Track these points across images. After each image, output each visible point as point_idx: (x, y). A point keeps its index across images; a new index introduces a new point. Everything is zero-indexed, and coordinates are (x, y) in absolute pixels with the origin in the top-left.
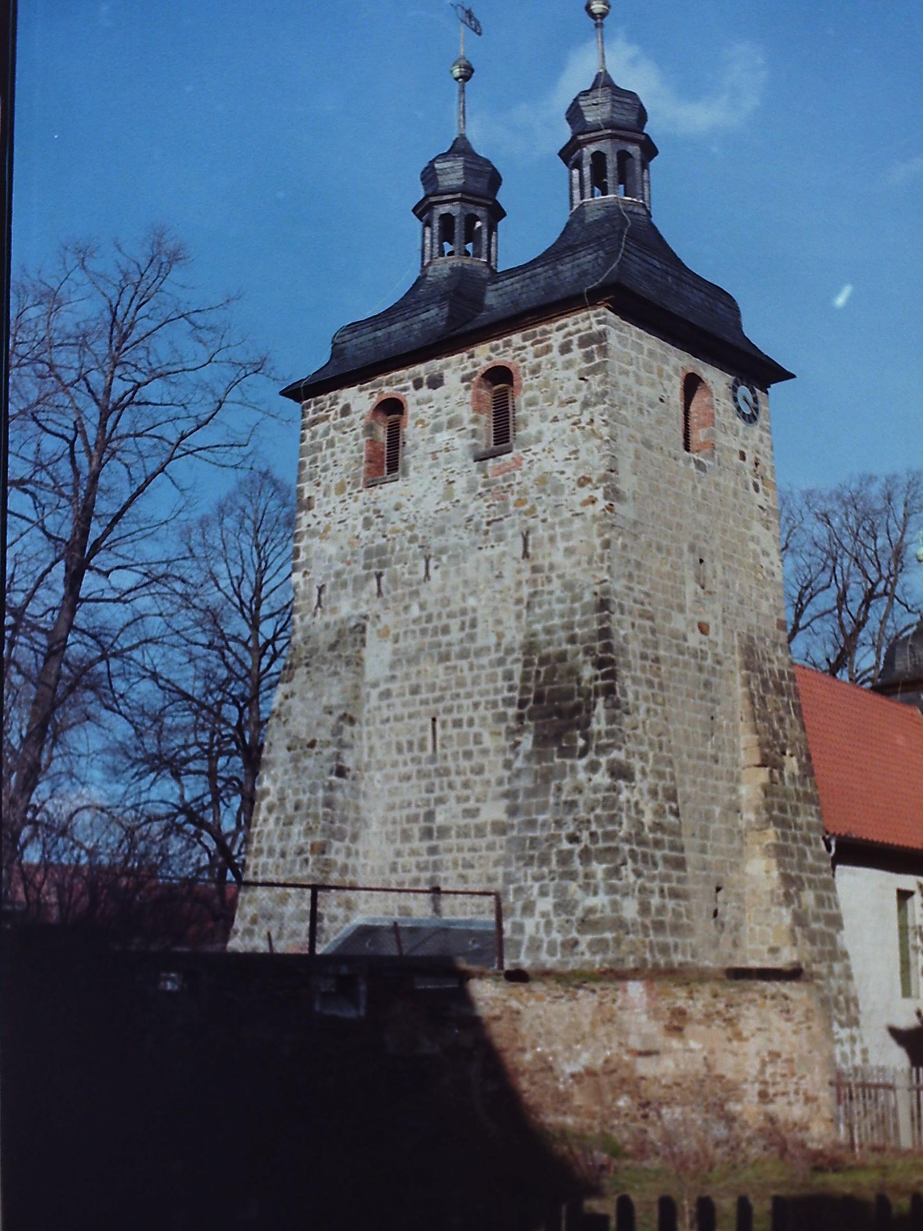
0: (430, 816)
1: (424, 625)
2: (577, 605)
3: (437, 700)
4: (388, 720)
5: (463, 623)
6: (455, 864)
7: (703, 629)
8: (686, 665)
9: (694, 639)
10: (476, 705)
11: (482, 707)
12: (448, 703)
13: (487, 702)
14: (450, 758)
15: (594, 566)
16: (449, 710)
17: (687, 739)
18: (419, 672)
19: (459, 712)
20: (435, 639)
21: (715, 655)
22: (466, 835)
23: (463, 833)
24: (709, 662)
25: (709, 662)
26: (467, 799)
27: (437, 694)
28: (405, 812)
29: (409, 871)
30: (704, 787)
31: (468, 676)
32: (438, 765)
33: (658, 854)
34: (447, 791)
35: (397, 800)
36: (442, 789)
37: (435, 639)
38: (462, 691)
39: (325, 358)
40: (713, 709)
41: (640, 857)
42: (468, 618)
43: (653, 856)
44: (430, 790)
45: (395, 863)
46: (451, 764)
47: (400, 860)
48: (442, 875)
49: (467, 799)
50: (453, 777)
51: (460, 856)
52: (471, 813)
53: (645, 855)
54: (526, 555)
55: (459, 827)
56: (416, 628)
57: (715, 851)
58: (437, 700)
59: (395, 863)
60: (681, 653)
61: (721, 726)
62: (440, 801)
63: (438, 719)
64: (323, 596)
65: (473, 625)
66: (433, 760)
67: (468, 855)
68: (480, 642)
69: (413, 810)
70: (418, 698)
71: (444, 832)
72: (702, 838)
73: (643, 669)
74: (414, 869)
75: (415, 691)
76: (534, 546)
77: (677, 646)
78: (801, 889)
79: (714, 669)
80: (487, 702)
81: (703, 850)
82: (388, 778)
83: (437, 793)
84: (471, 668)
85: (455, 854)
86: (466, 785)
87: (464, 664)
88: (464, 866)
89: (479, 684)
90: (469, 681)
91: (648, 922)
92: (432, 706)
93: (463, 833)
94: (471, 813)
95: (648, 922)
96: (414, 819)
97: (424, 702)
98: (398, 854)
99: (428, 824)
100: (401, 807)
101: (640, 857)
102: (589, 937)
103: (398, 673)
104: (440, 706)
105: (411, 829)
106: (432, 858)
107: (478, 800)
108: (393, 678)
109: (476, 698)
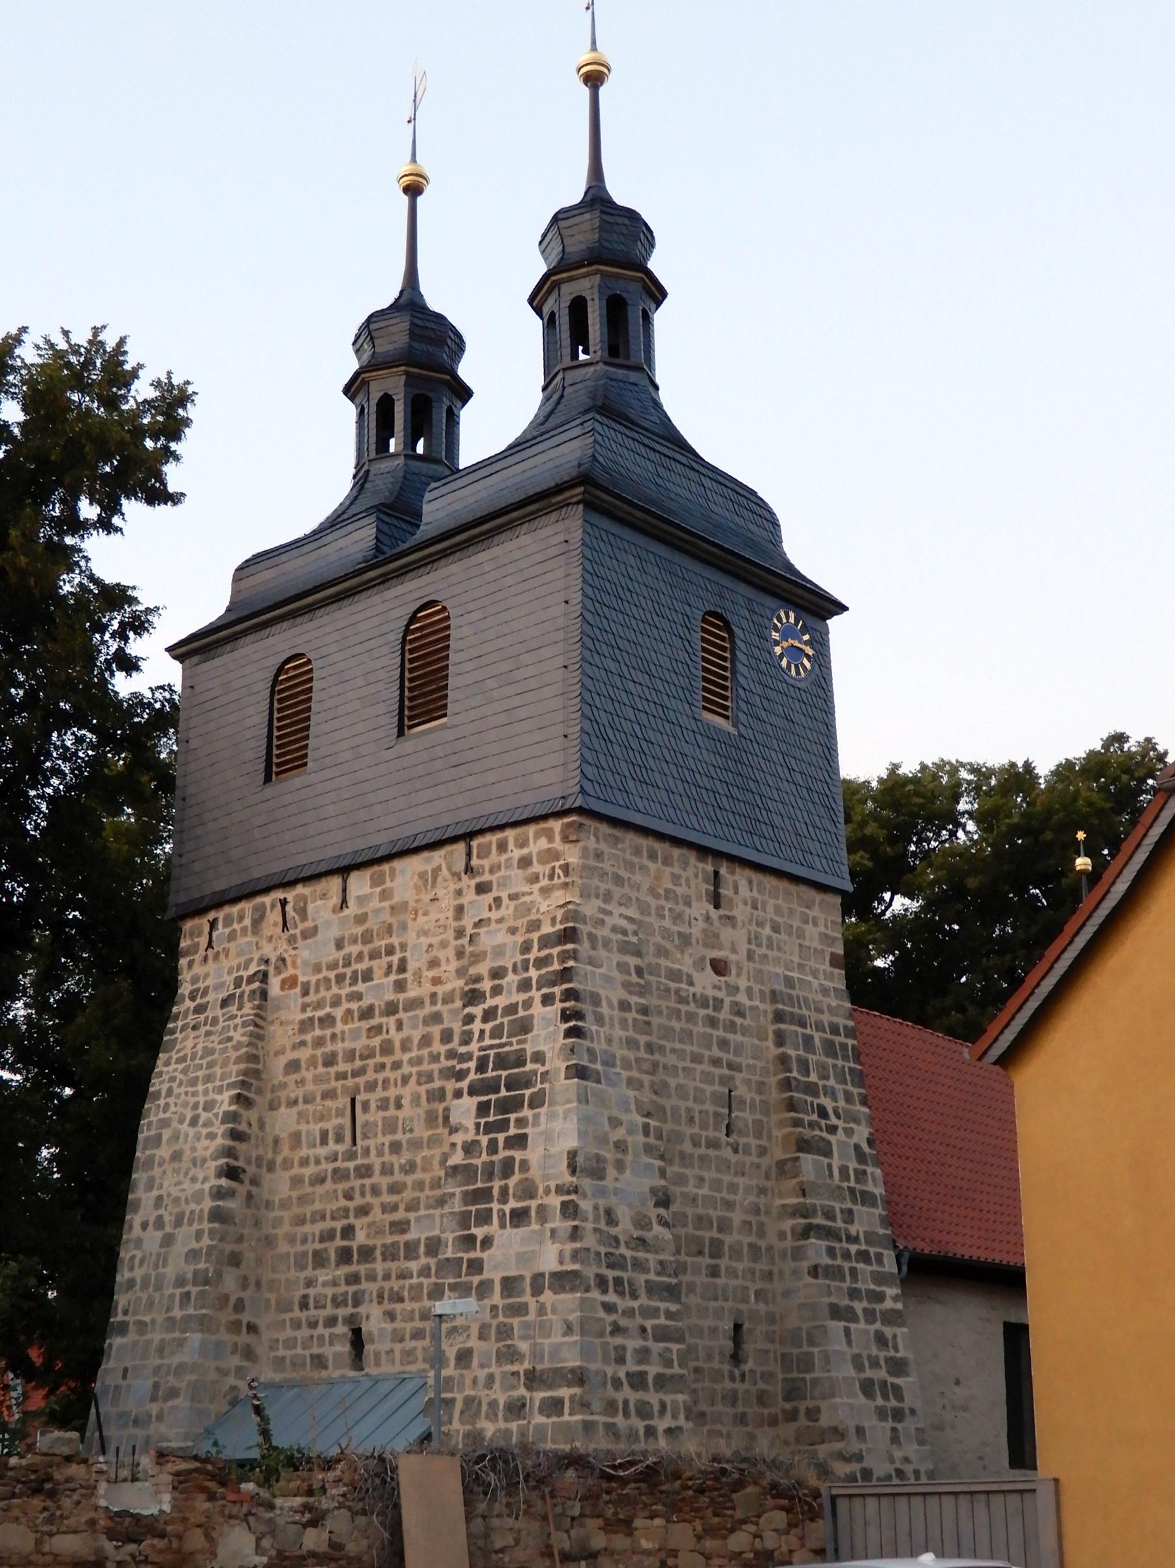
0: (348, 1232)
1: (341, 970)
2: (535, 936)
3: (356, 1074)
4: (295, 1102)
5: (390, 966)
6: (380, 1297)
7: (719, 968)
8: (691, 1017)
9: (706, 981)
10: (405, 1080)
11: (413, 1080)
12: (370, 1075)
13: (419, 1074)
14: (373, 1152)
15: (556, 881)
16: (371, 1087)
17: (691, 1120)
18: (334, 1036)
19: (384, 1089)
20: (354, 988)
21: (736, 1004)
22: (394, 1257)
23: (390, 1254)
24: (724, 1015)
25: (724, 1015)
26: (395, 1208)
27: (358, 1063)
28: (319, 1227)
29: (324, 1307)
30: (716, 1185)
31: (396, 1037)
32: (359, 1162)
33: (641, 1278)
34: (369, 1198)
35: (308, 1210)
36: (363, 1194)
37: (354, 988)
38: (388, 1060)
39: (222, 611)
40: (732, 1078)
41: (611, 1284)
42: (395, 959)
43: (630, 1284)
44: (348, 1196)
45: (305, 1297)
46: (375, 1160)
47: (311, 1292)
48: (362, 1310)
49: (395, 1208)
50: (376, 1179)
51: (387, 1285)
52: (401, 1227)
53: (618, 1282)
54: (469, 870)
55: (384, 1245)
56: (332, 975)
57: (732, 1273)
58: (356, 1074)
59: (305, 1297)
60: (682, 1000)
61: (744, 1102)
62: (363, 1211)
63: (358, 1098)
64: (214, 934)
65: (402, 968)
66: (351, 1156)
67: (395, 1284)
68: (412, 993)
69: (328, 1224)
70: (333, 1070)
71: (366, 1253)
72: (712, 1256)
73: (624, 1023)
74: (329, 1305)
75: (330, 1061)
76: (478, 857)
77: (677, 992)
78: (49, 1479)
79: (733, 1023)
80: (419, 1074)
81: (714, 1272)
82: (297, 1181)
83: (358, 1201)
84: (400, 1026)
85: (380, 1283)
86: (394, 1189)
87: (391, 1021)
88: (391, 1300)
89: (410, 1050)
90: (397, 1045)
91: (622, 1375)
92: (350, 1082)
93: (390, 1254)
94: (401, 1227)
95: (622, 1375)
96: (328, 1236)
97: (342, 1076)
98: (310, 1283)
99: (345, 1243)
100: (313, 1221)
101: (611, 1284)
102: (540, 1395)
103: (308, 1037)
104: (361, 1080)
105: (326, 1250)
106: (351, 1289)
107: (408, 1209)
108: (303, 1043)
109: (406, 1069)
